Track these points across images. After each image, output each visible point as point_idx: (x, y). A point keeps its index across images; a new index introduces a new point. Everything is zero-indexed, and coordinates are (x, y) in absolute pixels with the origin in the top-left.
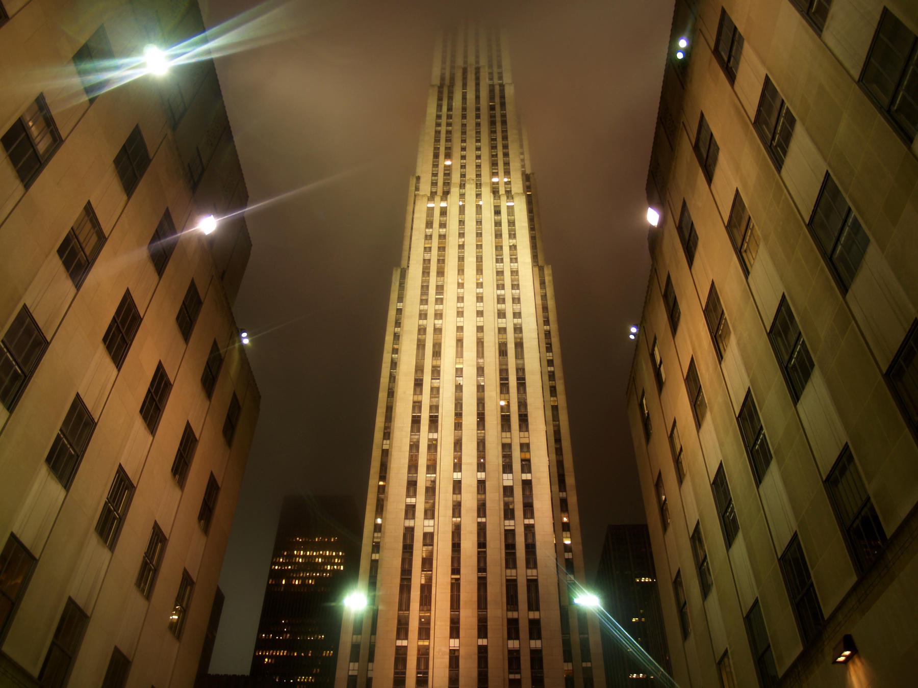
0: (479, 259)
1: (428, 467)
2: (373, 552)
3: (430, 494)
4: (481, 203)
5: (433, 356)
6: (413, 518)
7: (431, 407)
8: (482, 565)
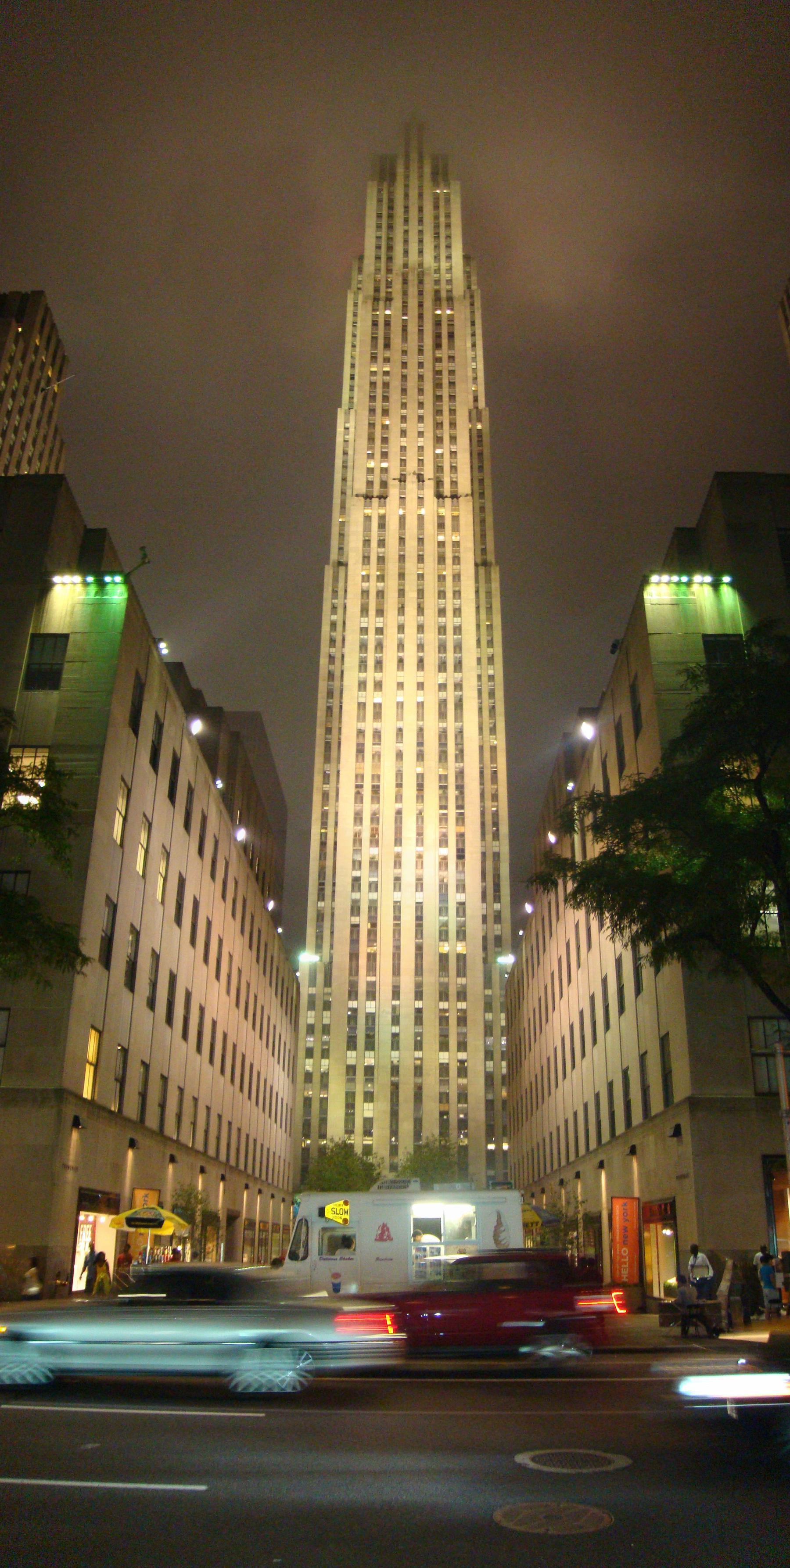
0: (421, 593)
1: (371, 842)
2: (319, 900)
3: (374, 867)
4: (423, 512)
5: (374, 718)
6: (359, 890)
7: (373, 776)
8: (419, 914)
